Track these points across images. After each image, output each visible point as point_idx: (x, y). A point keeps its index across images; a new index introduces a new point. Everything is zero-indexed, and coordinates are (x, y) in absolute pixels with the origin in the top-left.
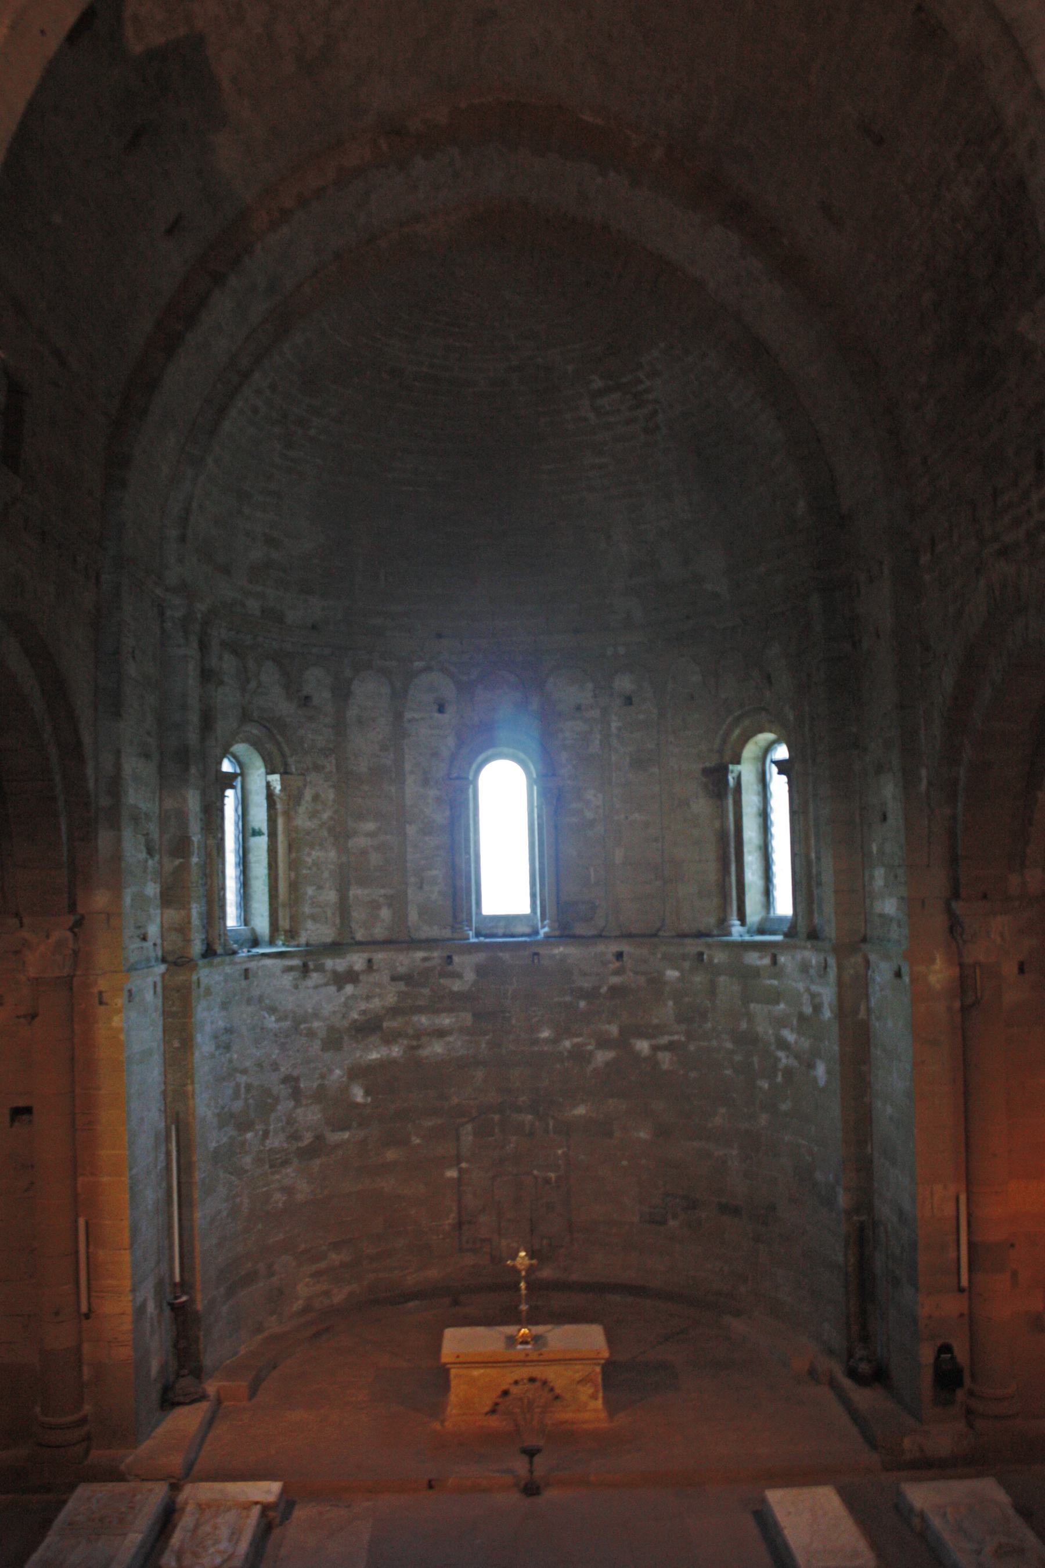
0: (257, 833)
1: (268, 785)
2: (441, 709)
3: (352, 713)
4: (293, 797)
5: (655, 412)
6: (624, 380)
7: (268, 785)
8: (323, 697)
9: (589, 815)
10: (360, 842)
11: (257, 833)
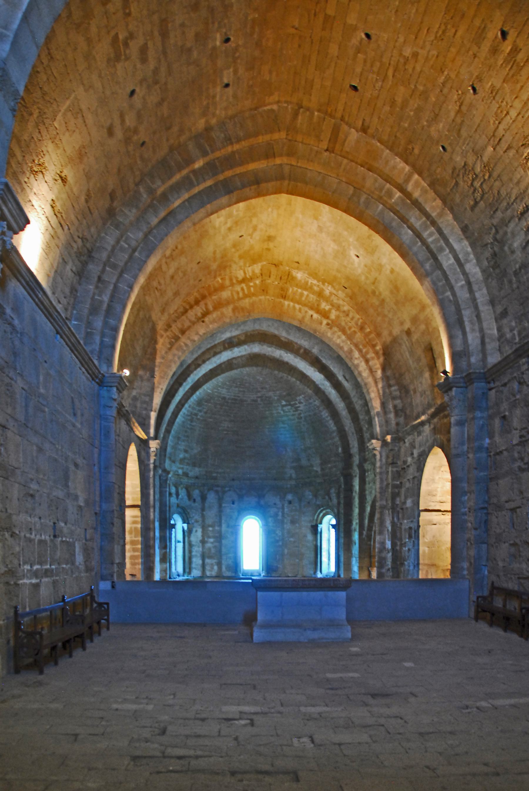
0: (179, 542)
1: (183, 527)
2: (233, 503)
3: (206, 505)
4: (190, 531)
5: (300, 414)
6: (292, 403)
7: (183, 527)
8: (198, 499)
9: (277, 538)
10: (208, 545)
11: (179, 542)
